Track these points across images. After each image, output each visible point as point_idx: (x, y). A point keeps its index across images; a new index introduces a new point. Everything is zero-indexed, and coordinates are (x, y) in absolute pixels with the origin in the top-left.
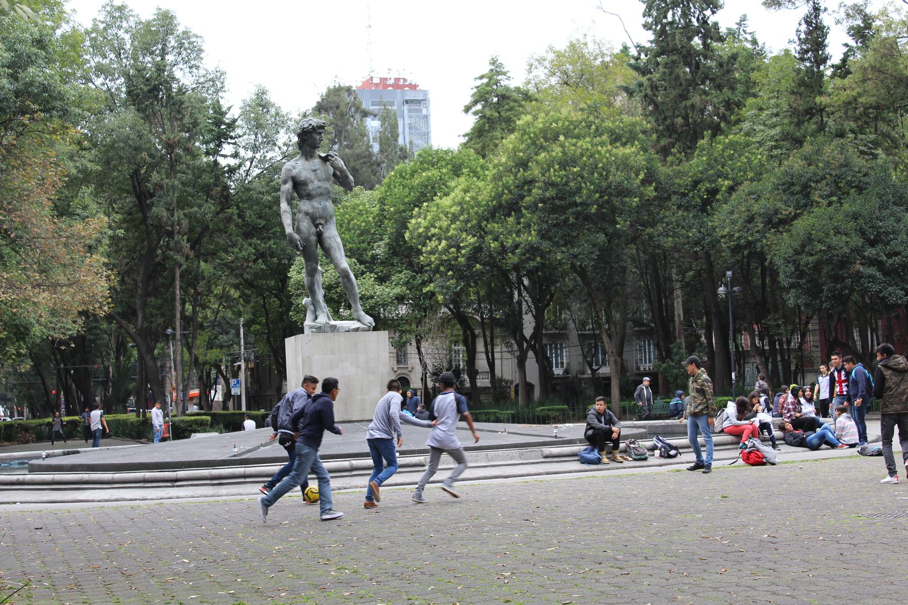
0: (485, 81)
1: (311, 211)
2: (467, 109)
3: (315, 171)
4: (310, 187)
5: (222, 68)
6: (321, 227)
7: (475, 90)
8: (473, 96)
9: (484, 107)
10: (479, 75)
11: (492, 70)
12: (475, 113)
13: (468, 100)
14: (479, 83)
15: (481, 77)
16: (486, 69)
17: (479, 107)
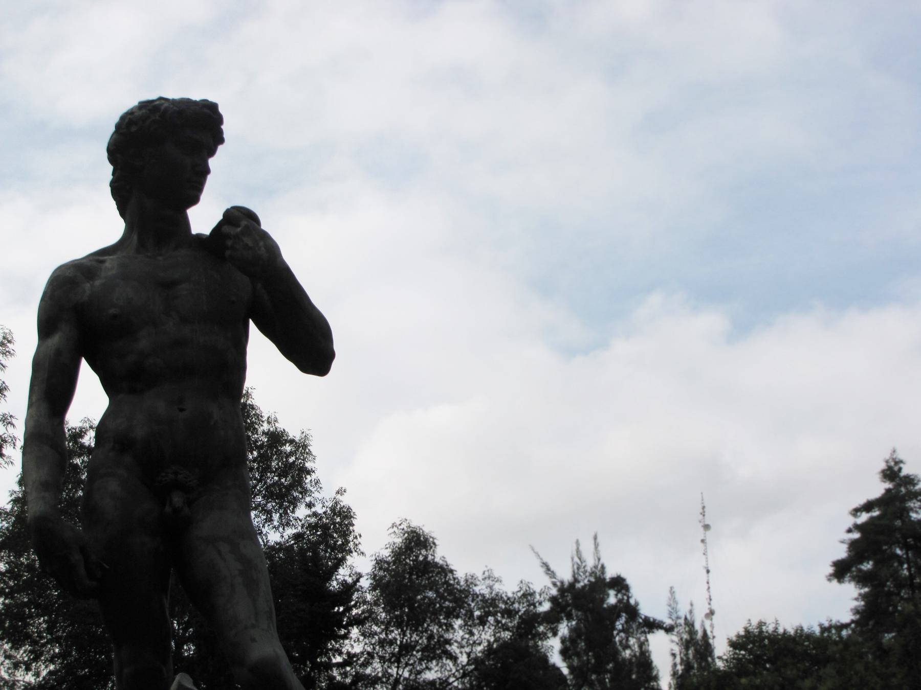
0: (876, 513)
1: (140, 432)
2: (841, 571)
3: (168, 285)
4: (144, 343)
5: (345, 501)
6: (177, 499)
7: (856, 535)
8: (853, 545)
9: (875, 565)
10: (862, 501)
11: (888, 491)
12: (862, 579)
13: (842, 553)
14: (864, 517)
15: (868, 507)
16: (878, 489)
17: (867, 566)
